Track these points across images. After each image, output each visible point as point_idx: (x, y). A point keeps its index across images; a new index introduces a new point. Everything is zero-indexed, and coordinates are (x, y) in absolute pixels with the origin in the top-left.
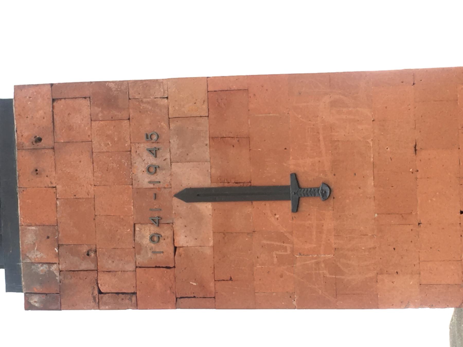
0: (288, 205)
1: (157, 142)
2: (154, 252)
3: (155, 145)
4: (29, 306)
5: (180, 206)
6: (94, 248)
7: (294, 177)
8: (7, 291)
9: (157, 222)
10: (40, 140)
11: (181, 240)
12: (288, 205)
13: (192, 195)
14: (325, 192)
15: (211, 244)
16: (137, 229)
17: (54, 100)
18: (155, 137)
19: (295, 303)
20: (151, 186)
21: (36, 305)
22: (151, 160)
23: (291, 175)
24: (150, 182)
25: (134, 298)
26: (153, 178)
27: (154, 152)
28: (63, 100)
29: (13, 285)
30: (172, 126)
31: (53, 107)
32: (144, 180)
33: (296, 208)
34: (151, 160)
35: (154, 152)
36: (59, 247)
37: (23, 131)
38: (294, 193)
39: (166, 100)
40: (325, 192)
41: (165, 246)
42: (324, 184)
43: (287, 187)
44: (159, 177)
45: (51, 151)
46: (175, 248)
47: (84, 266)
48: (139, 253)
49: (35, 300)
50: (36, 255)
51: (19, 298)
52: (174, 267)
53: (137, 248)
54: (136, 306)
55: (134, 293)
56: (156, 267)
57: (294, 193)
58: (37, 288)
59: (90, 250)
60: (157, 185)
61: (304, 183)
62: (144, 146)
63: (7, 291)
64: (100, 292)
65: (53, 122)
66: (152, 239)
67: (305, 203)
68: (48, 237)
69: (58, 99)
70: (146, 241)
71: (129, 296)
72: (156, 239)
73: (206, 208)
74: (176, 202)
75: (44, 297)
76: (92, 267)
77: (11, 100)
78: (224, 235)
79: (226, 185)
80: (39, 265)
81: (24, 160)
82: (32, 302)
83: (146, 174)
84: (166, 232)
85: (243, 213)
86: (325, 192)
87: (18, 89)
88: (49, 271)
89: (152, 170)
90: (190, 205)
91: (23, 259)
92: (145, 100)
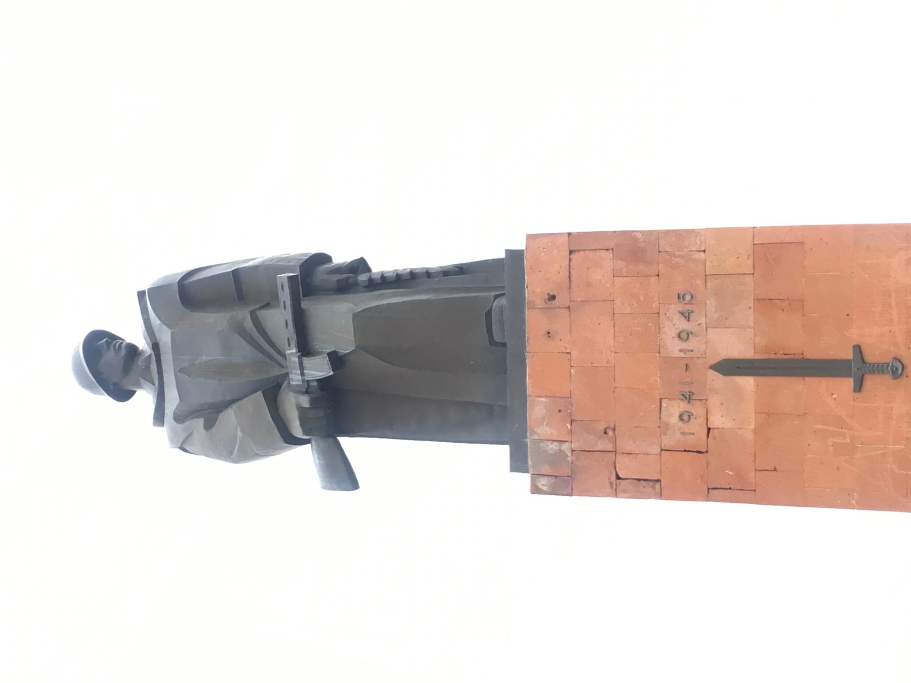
0: (849, 383)
1: (690, 303)
2: (683, 433)
3: (688, 307)
4: (535, 490)
5: (716, 379)
6: (612, 426)
7: (858, 349)
9: (688, 398)
10: (553, 298)
11: (717, 421)
12: (849, 383)
13: (731, 367)
14: (895, 369)
15: (752, 426)
16: (664, 405)
17: (571, 252)
18: (688, 298)
19: (854, 502)
20: (682, 355)
21: (545, 488)
22: (683, 325)
23: (854, 346)
24: (681, 351)
25: (658, 486)
26: (684, 346)
27: (686, 315)
28: (581, 252)
29: (518, 463)
30: (708, 284)
31: (570, 260)
32: (674, 347)
33: (859, 387)
34: (683, 325)
35: (687, 315)
36: (572, 422)
37: (535, 286)
38: (857, 368)
39: (702, 254)
40: (895, 369)
41: (697, 427)
42: (896, 359)
43: (849, 361)
44: (692, 344)
45: (566, 311)
46: (709, 429)
47: (600, 447)
48: (665, 434)
49: (543, 483)
50: (544, 431)
52: (707, 452)
53: (663, 428)
54: (660, 496)
55: (658, 481)
56: (685, 451)
57: (857, 368)
58: (546, 469)
59: (608, 428)
60: (689, 355)
61: (871, 356)
62: (675, 308)
64: (618, 478)
65: (570, 278)
66: (681, 417)
67: (871, 382)
68: (560, 411)
69: (575, 251)
70: (674, 419)
71: (652, 484)
72: (686, 417)
73: (748, 383)
74: (712, 374)
75: (552, 480)
76: (610, 447)
77: (522, 251)
78: (768, 416)
79: (773, 356)
80: (549, 443)
81: (535, 321)
82: (539, 485)
83: (677, 341)
84: (697, 409)
85: (792, 390)
86: (897, 369)
87: (530, 237)
88: (560, 450)
89: (684, 336)
90: (728, 378)
91: (531, 435)
92: (677, 253)
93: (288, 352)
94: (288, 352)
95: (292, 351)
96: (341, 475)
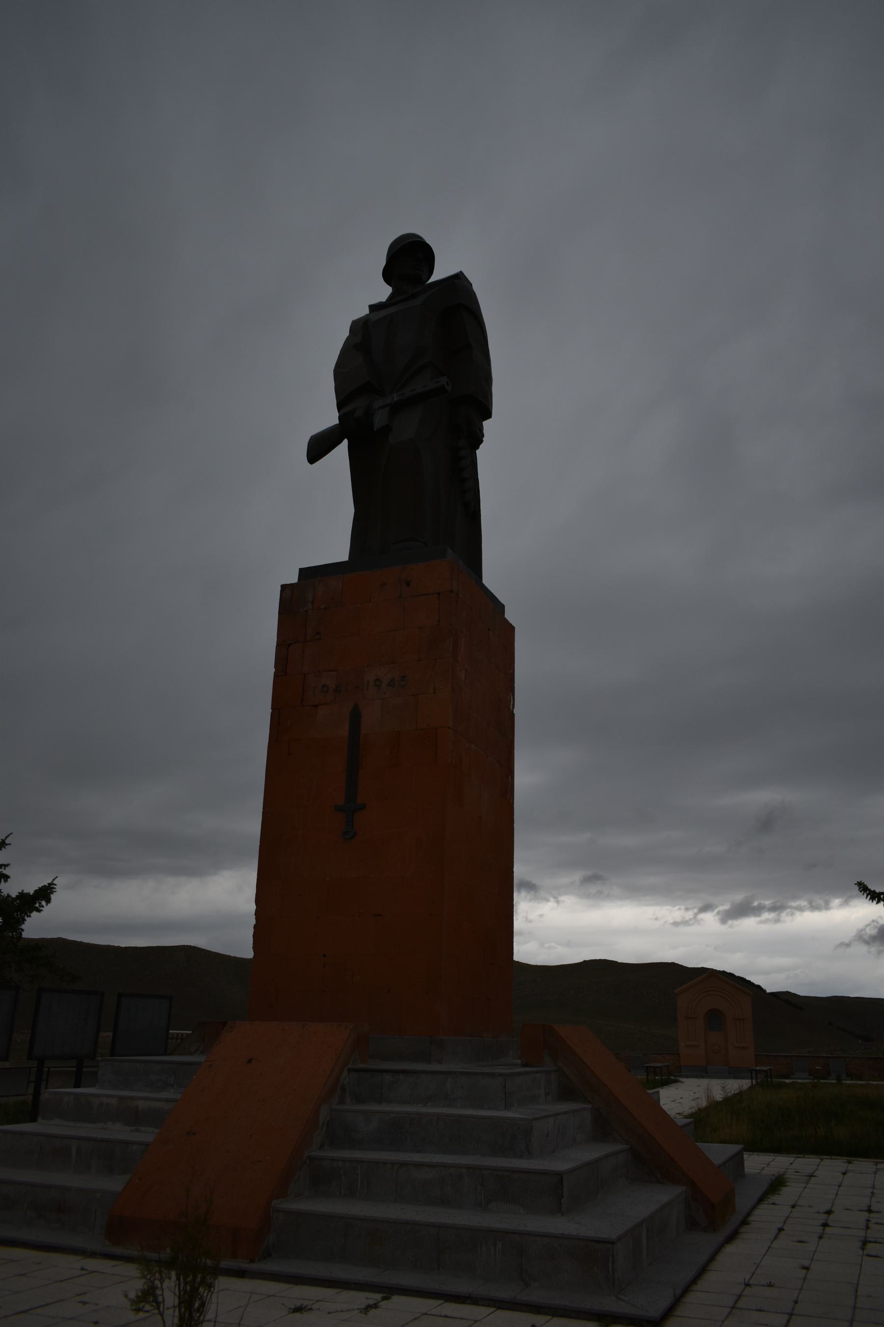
4: (284, 587)
8: (301, 570)
10: (408, 584)
13: (356, 718)
17: (438, 594)
46: (316, 706)
51: (294, 579)
54: (276, 675)
63: (301, 570)
64: (289, 645)
66: (324, 686)
93: (395, 395)
94: (395, 395)
95: (396, 397)
96: (319, 448)
